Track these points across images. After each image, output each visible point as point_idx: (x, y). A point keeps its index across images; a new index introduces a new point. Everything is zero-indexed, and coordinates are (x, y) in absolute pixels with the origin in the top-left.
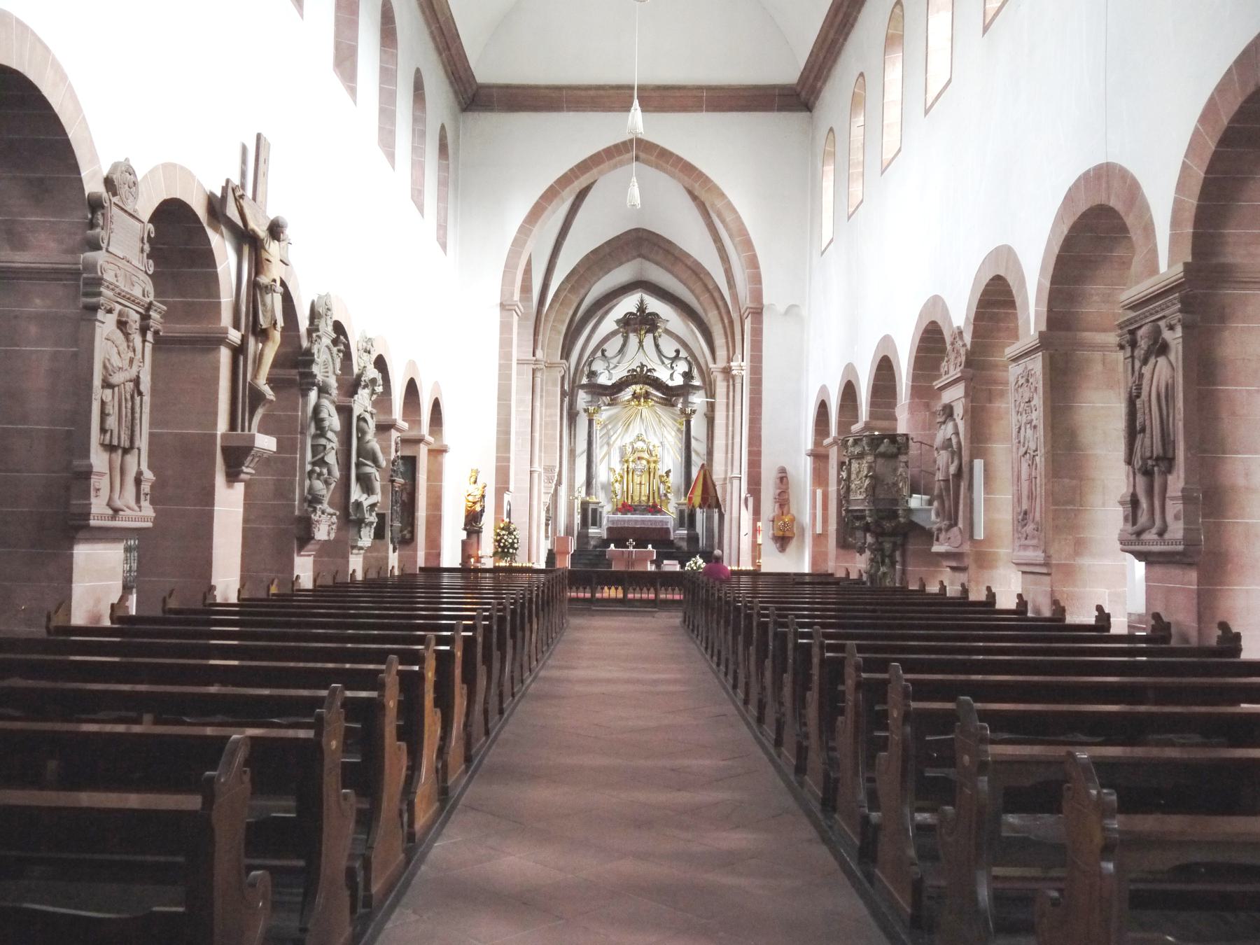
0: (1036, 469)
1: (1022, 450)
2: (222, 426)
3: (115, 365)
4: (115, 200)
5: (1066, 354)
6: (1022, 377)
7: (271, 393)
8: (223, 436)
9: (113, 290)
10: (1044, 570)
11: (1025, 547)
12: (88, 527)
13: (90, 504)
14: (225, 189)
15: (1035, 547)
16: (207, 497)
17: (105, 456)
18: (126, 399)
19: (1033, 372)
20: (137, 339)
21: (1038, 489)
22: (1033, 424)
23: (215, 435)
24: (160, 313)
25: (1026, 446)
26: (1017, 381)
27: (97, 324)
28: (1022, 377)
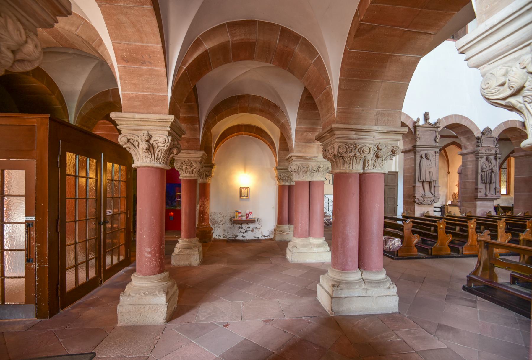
4: (484, 136)
17: (484, 185)
20: (493, 161)
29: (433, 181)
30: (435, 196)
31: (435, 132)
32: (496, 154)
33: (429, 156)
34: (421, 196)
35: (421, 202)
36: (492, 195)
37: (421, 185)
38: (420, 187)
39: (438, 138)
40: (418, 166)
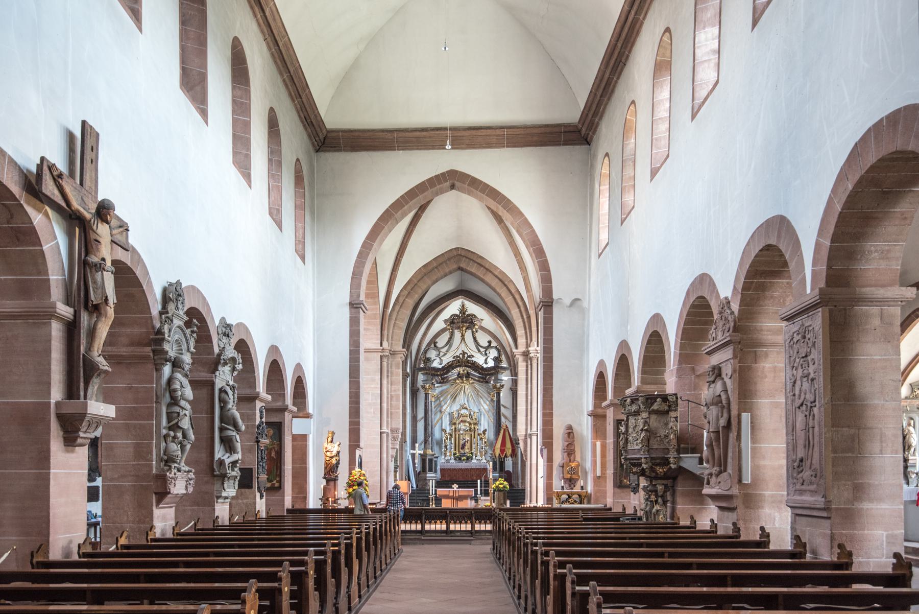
0: (814, 419)
1: (798, 402)
2: (57, 394)
5: (845, 309)
6: (798, 334)
7: (104, 362)
8: (58, 404)
10: (825, 514)
11: (801, 492)
14: (40, 167)
15: (814, 493)
16: (43, 460)
19: (810, 328)
21: (817, 439)
22: (811, 377)
23: (50, 403)
25: (802, 398)
26: (792, 339)
28: (798, 334)
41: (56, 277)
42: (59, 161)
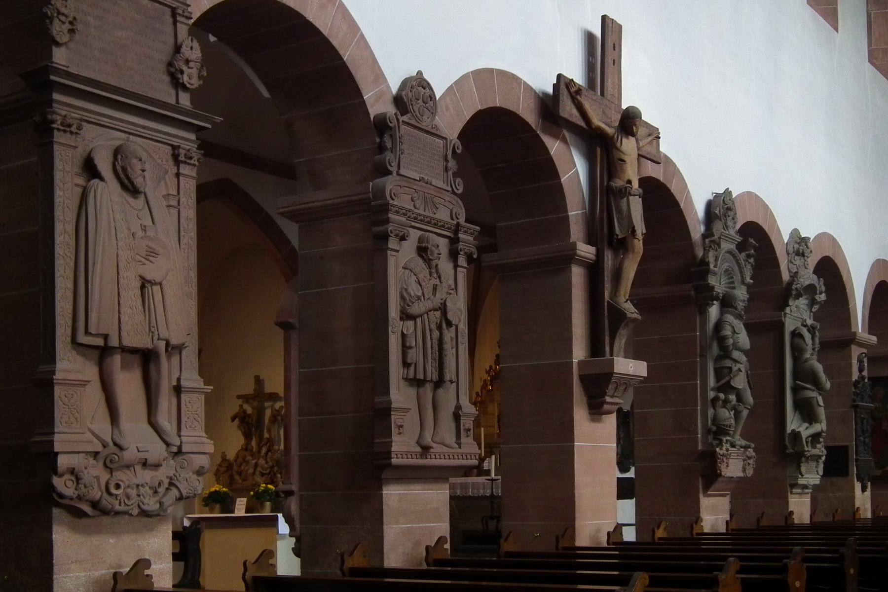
2: (579, 352)
3: (412, 294)
4: (405, 118)
8: (580, 363)
9: (404, 214)
12: (390, 465)
13: (391, 442)
14: (556, 87)
16: (567, 432)
17: (412, 392)
18: (430, 330)
20: (445, 266)
24: (472, 234)
27: (389, 252)
29: (168, 344)
30: (179, 452)
31: (170, 20)
32: (457, 228)
33: (138, 166)
34: (96, 454)
35: (96, 494)
36: (445, 449)
37: (90, 372)
38: (83, 384)
39: (187, 62)
40: (71, 228)
41: (575, 212)
42: (577, 74)
